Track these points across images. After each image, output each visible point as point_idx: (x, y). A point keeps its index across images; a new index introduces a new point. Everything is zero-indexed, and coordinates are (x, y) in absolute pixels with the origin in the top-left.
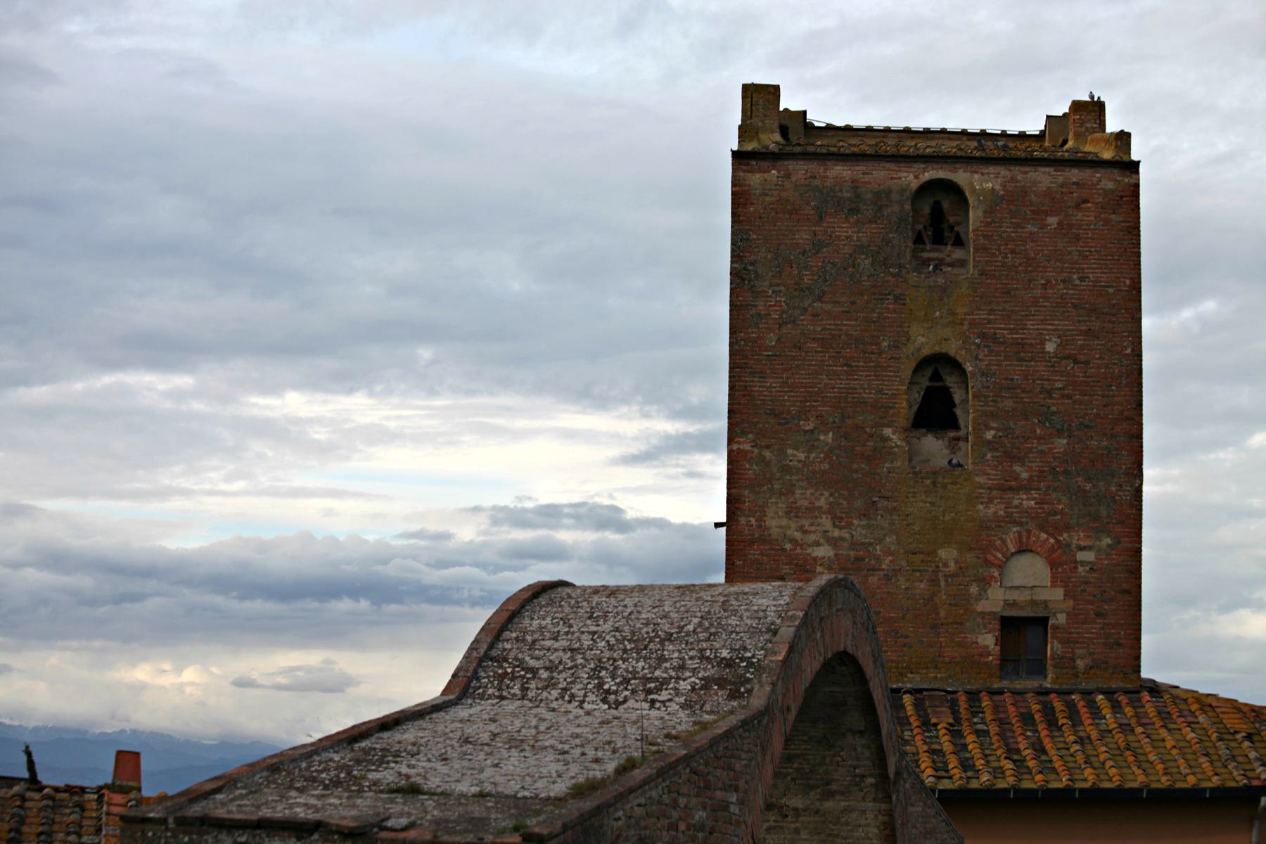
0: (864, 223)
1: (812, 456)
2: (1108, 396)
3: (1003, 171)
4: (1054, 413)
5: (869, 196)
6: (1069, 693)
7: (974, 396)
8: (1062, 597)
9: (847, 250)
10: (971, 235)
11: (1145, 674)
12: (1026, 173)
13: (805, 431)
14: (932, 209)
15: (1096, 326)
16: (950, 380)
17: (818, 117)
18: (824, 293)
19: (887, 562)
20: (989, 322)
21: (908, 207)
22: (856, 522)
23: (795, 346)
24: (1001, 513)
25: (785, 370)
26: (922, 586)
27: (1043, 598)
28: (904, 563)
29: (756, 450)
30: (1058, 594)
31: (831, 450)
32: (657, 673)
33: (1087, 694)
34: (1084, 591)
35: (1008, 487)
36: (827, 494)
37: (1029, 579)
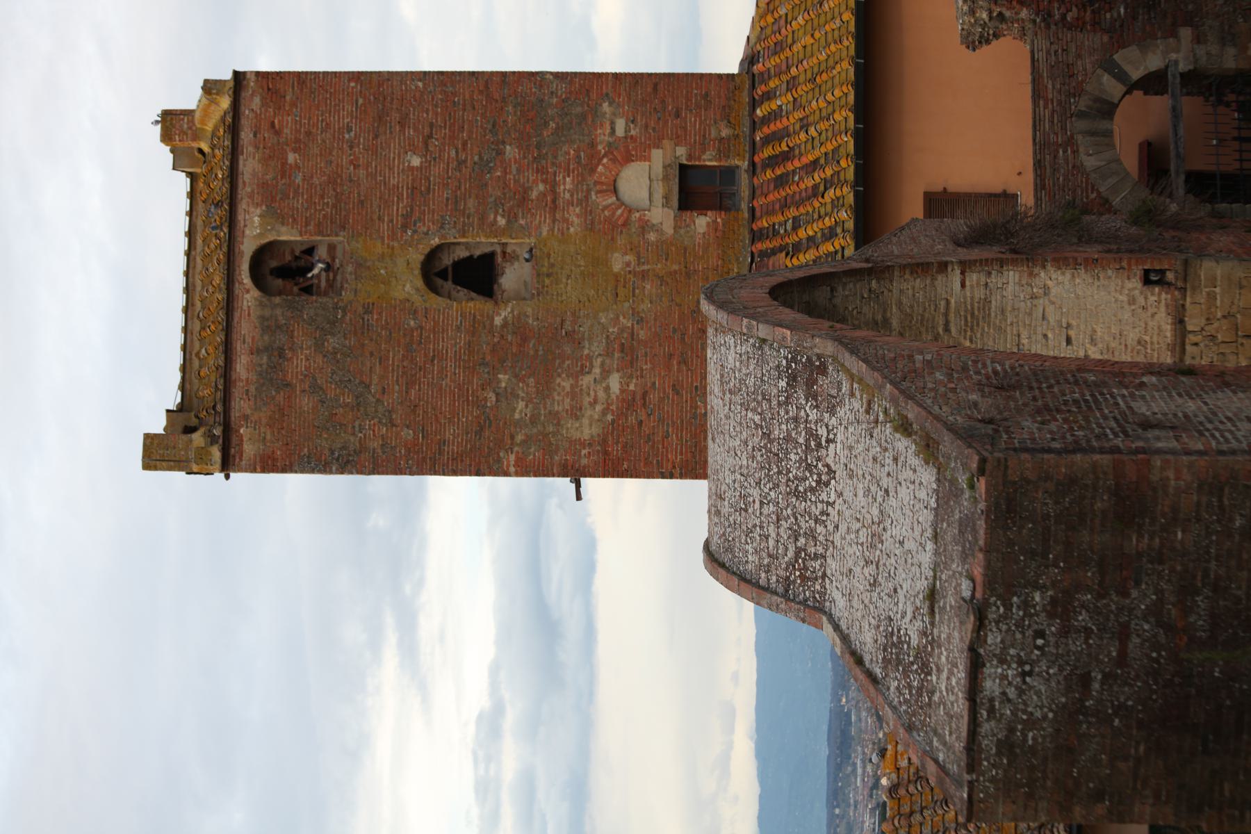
0: (294, 343)
1: (522, 394)
2: (464, 105)
3: (242, 206)
4: (481, 158)
5: (266, 338)
6: (754, 142)
7: (464, 236)
8: (660, 151)
9: (319, 359)
10: (305, 238)
11: (734, 69)
12: (244, 183)
13: (497, 401)
14: (278, 277)
15: (396, 116)
16: (447, 260)
17: (173, 398)
18: (362, 382)
19: (625, 321)
20: (392, 221)
21: (277, 300)
22: (586, 352)
23: (414, 411)
24: (577, 210)
25: (437, 420)
26: (648, 287)
27: (661, 170)
28: (626, 305)
29: (516, 449)
30: (657, 154)
31: (516, 376)
32: (801, 440)
33: (754, 126)
34: (654, 129)
35: (553, 204)
36: (558, 380)
37: (642, 184)
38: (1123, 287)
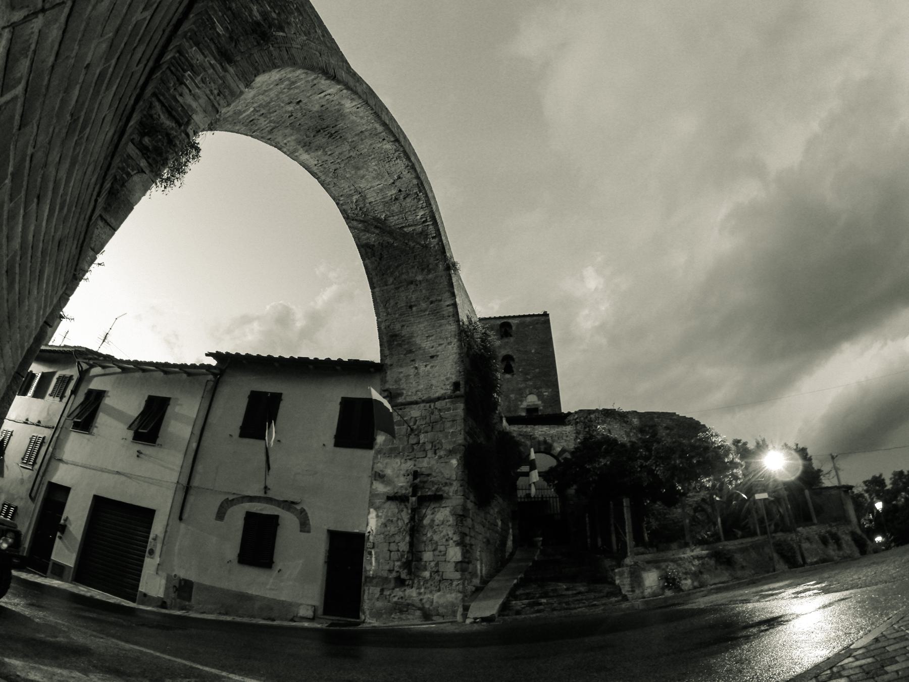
30: (540, 402)
35: (526, 380)
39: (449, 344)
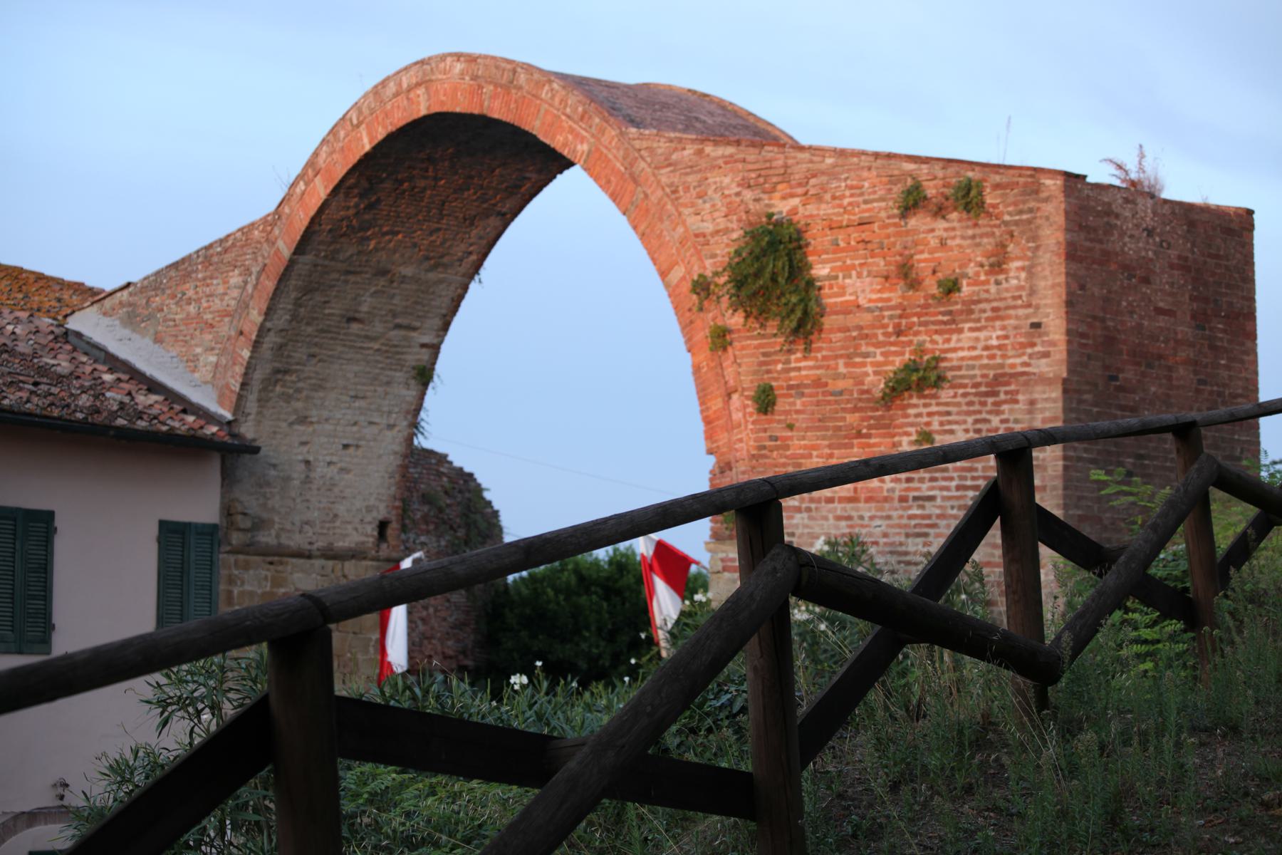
38: (381, 500)
39: (391, 427)
